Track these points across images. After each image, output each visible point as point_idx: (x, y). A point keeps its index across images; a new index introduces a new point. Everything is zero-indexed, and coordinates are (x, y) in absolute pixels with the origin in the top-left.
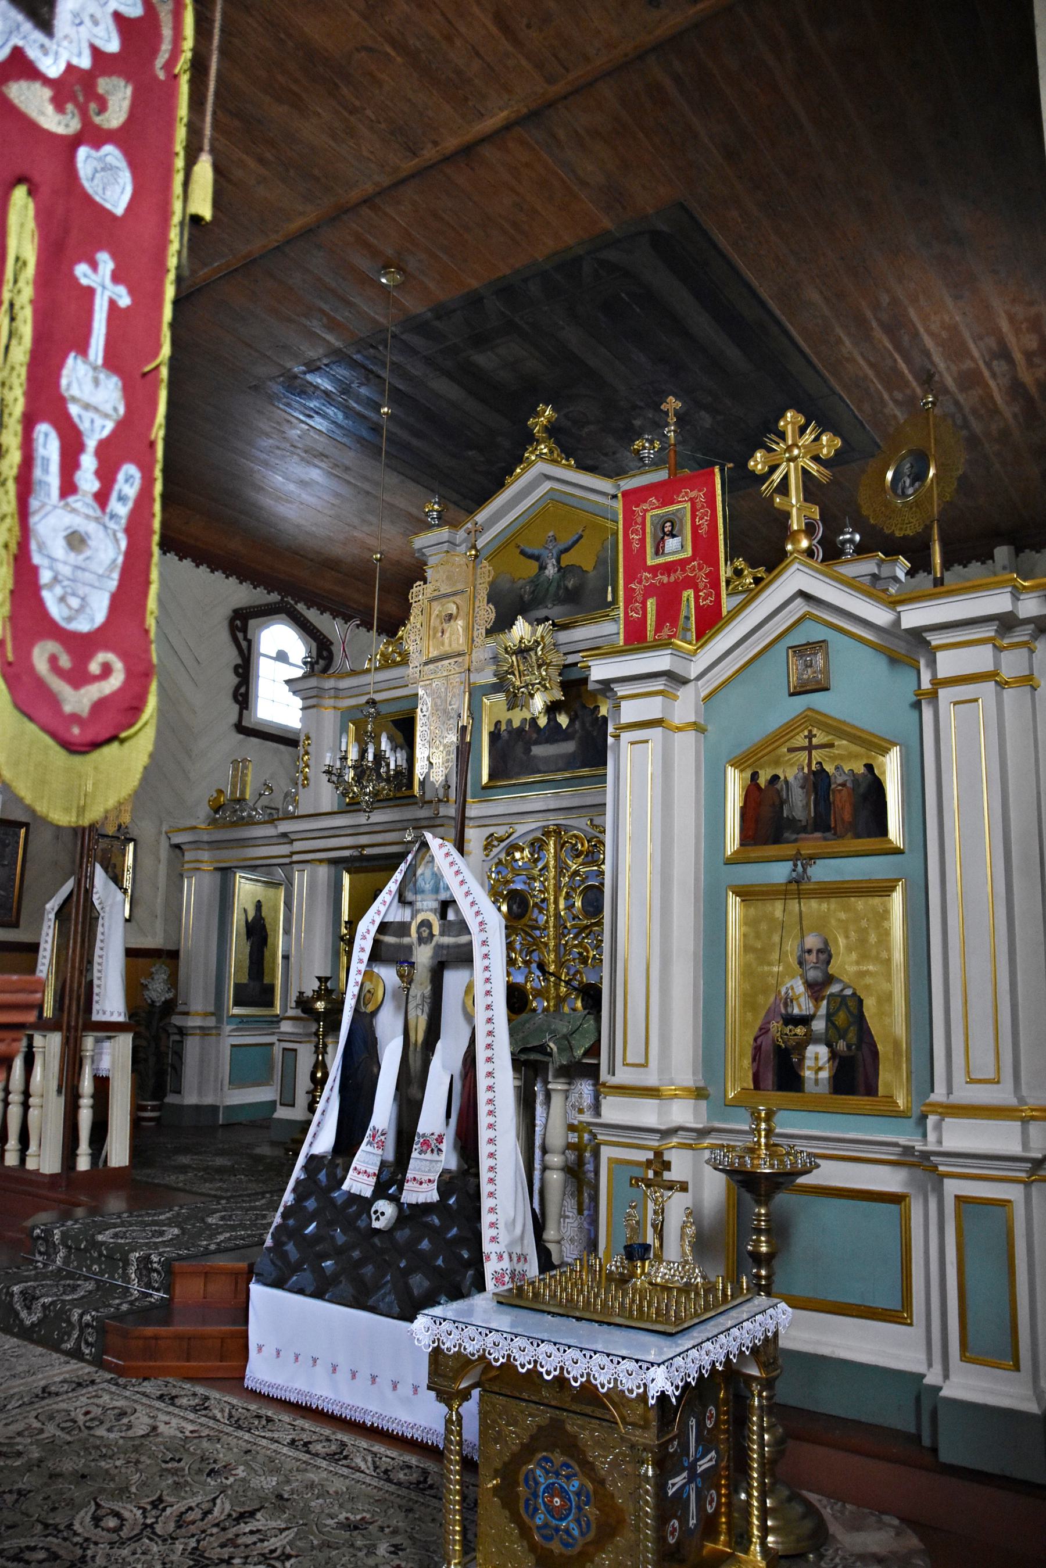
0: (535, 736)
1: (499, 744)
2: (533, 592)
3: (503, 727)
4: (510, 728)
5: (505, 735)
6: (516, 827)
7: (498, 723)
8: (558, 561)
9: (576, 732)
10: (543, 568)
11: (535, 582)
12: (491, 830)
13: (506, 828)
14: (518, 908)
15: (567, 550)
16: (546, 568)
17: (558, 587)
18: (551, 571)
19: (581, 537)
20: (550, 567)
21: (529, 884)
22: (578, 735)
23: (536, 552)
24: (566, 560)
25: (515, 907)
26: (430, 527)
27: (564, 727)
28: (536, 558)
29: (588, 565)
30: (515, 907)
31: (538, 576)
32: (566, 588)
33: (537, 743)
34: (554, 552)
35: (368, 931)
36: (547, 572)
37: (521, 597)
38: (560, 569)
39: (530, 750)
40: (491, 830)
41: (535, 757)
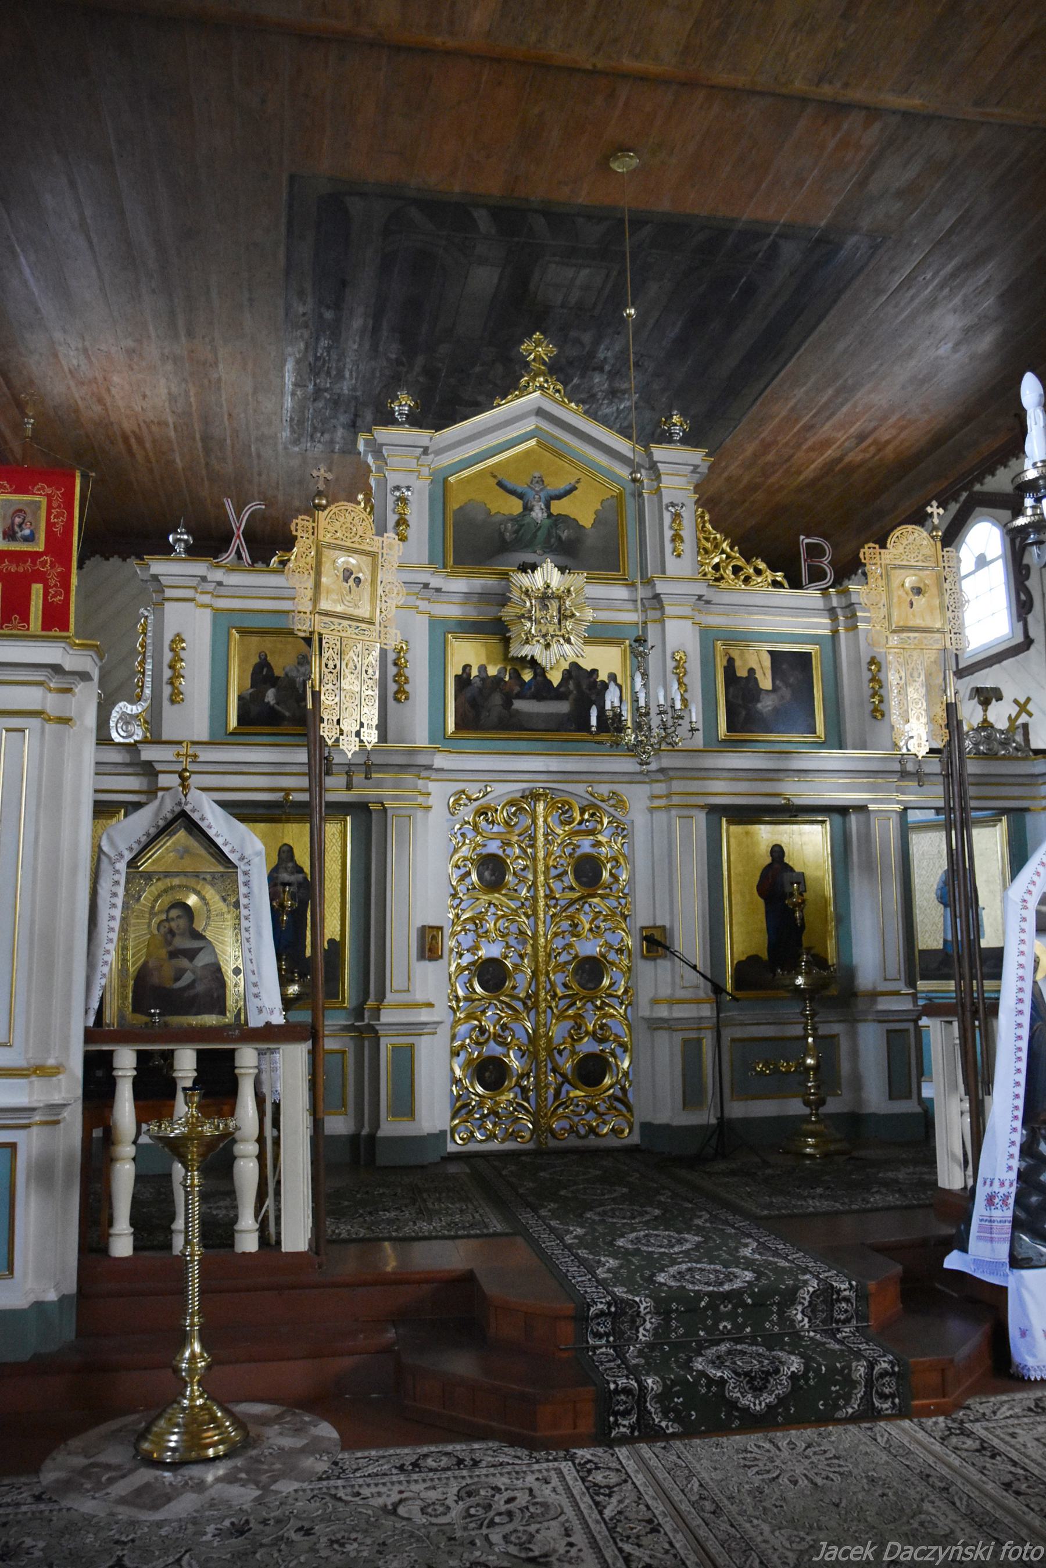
0: (517, 689)
1: (469, 692)
2: (517, 532)
3: (474, 672)
4: (483, 675)
5: (478, 683)
6: (495, 785)
7: (467, 668)
8: (548, 507)
9: (571, 692)
10: (528, 508)
11: (519, 521)
12: (460, 786)
13: (481, 785)
14: (493, 874)
15: (559, 497)
16: (532, 509)
17: (549, 535)
18: (538, 514)
19: (574, 488)
20: (537, 509)
21: (504, 850)
22: (571, 697)
23: (519, 490)
24: (557, 508)
25: (487, 874)
26: (394, 422)
27: (555, 685)
28: (521, 496)
29: (586, 520)
30: (487, 874)
31: (522, 515)
32: (559, 538)
33: (519, 696)
34: (542, 494)
35: (115, 895)
36: (533, 514)
37: (501, 534)
38: (550, 515)
39: (512, 704)
40: (460, 786)
41: (517, 711)
